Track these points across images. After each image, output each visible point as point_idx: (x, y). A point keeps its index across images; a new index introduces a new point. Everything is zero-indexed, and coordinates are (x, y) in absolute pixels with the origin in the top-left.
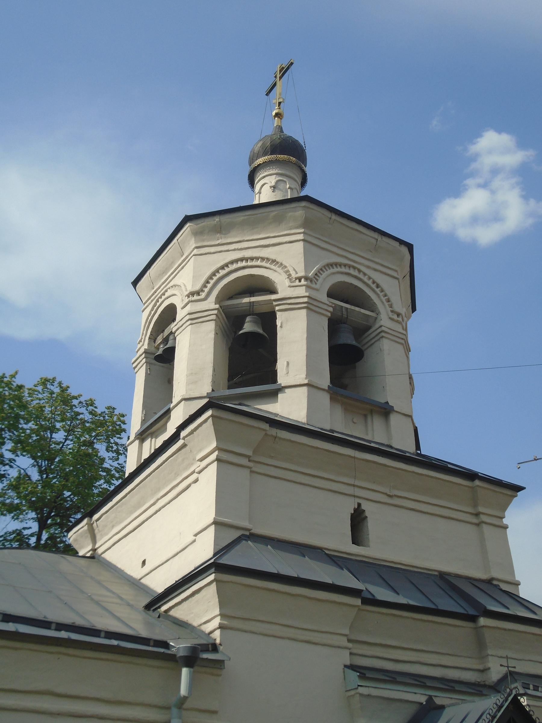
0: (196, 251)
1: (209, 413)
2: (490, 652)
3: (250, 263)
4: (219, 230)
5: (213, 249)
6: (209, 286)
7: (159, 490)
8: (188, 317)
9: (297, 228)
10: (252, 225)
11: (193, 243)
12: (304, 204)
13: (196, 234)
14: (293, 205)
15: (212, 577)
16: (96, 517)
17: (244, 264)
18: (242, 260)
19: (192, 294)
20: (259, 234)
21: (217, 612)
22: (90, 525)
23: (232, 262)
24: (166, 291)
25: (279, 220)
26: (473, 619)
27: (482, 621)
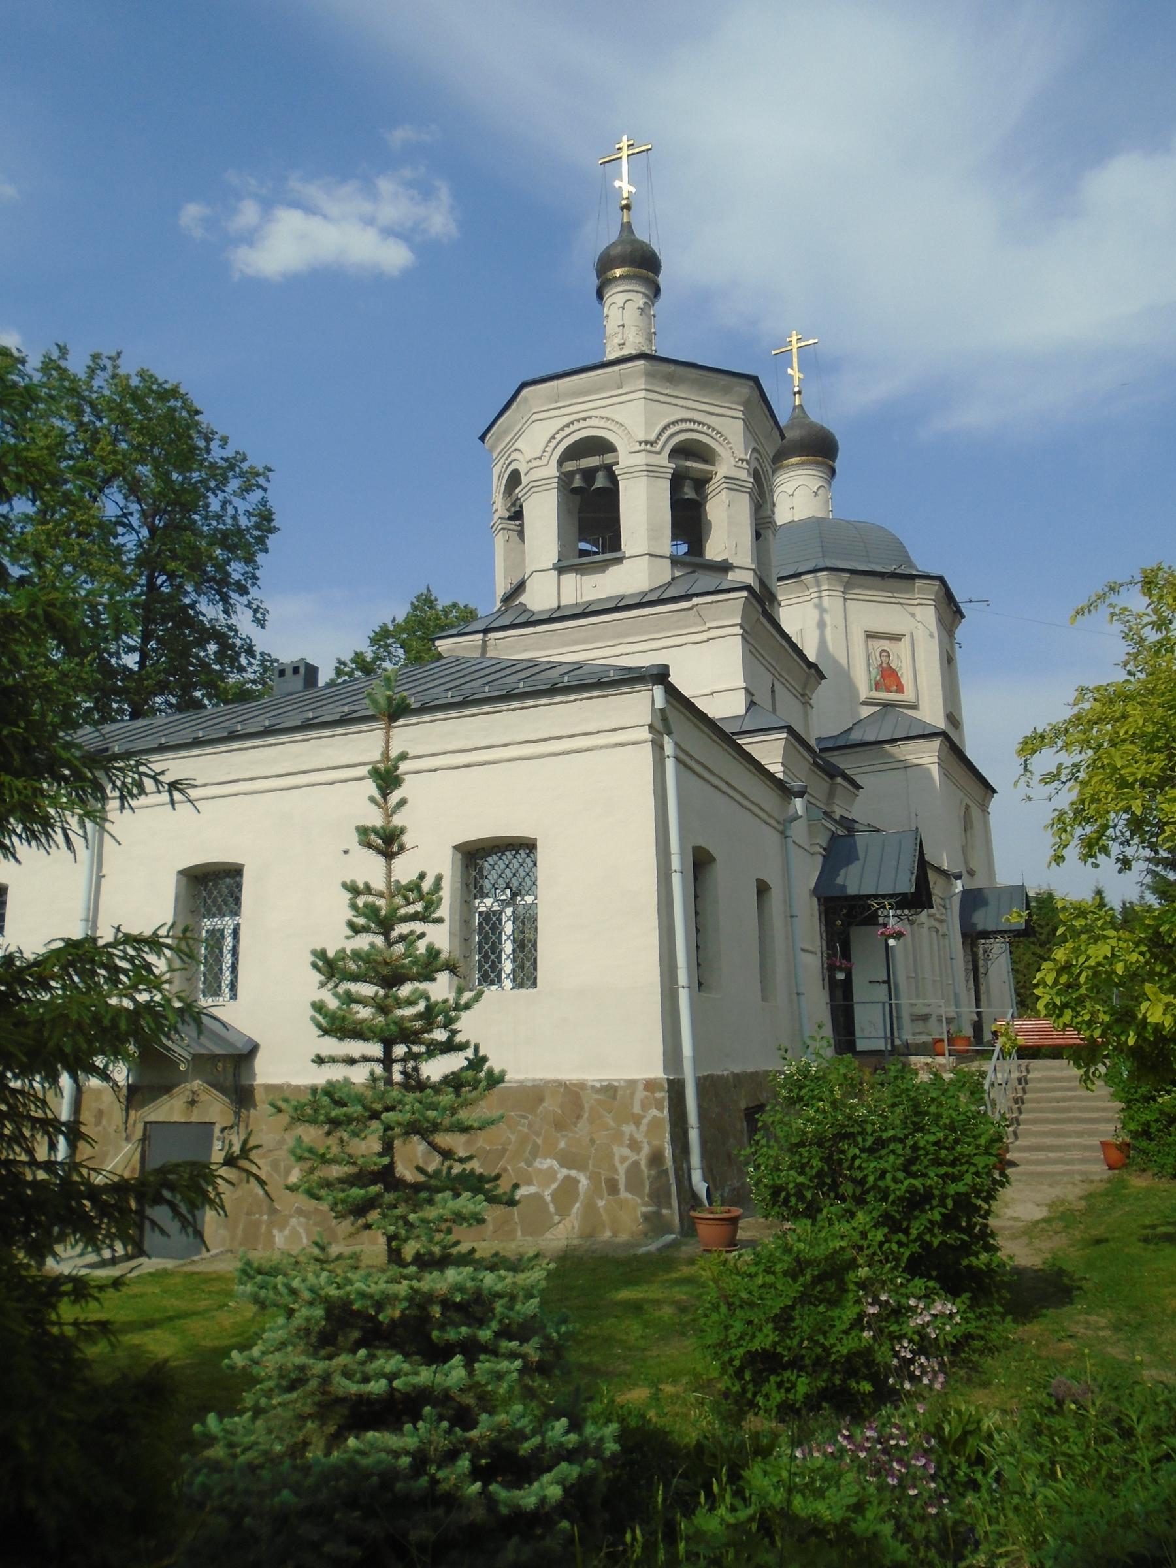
0: (643, 394)
1: (745, 594)
2: (837, 801)
3: (700, 428)
4: (670, 379)
5: (662, 398)
6: (663, 439)
7: (627, 635)
8: (645, 468)
9: (738, 404)
10: (702, 386)
11: (641, 383)
12: (751, 383)
13: (649, 375)
14: (743, 381)
15: (785, 735)
16: (491, 635)
17: (691, 426)
18: (690, 421)
19: (646, 443)
20: (704, 396)
21: (781, 760)
22: (484, 641)
23: (682, 420)
24: (590, 417)
25: (726, 390)
26: (832, 777)
27: (839, 780)
